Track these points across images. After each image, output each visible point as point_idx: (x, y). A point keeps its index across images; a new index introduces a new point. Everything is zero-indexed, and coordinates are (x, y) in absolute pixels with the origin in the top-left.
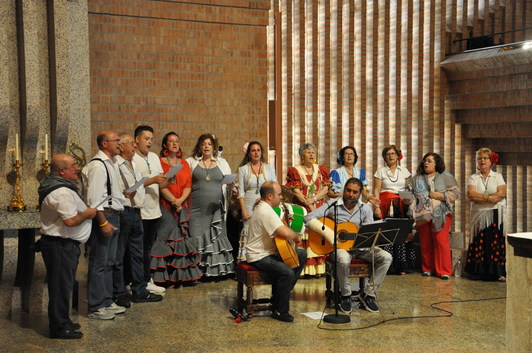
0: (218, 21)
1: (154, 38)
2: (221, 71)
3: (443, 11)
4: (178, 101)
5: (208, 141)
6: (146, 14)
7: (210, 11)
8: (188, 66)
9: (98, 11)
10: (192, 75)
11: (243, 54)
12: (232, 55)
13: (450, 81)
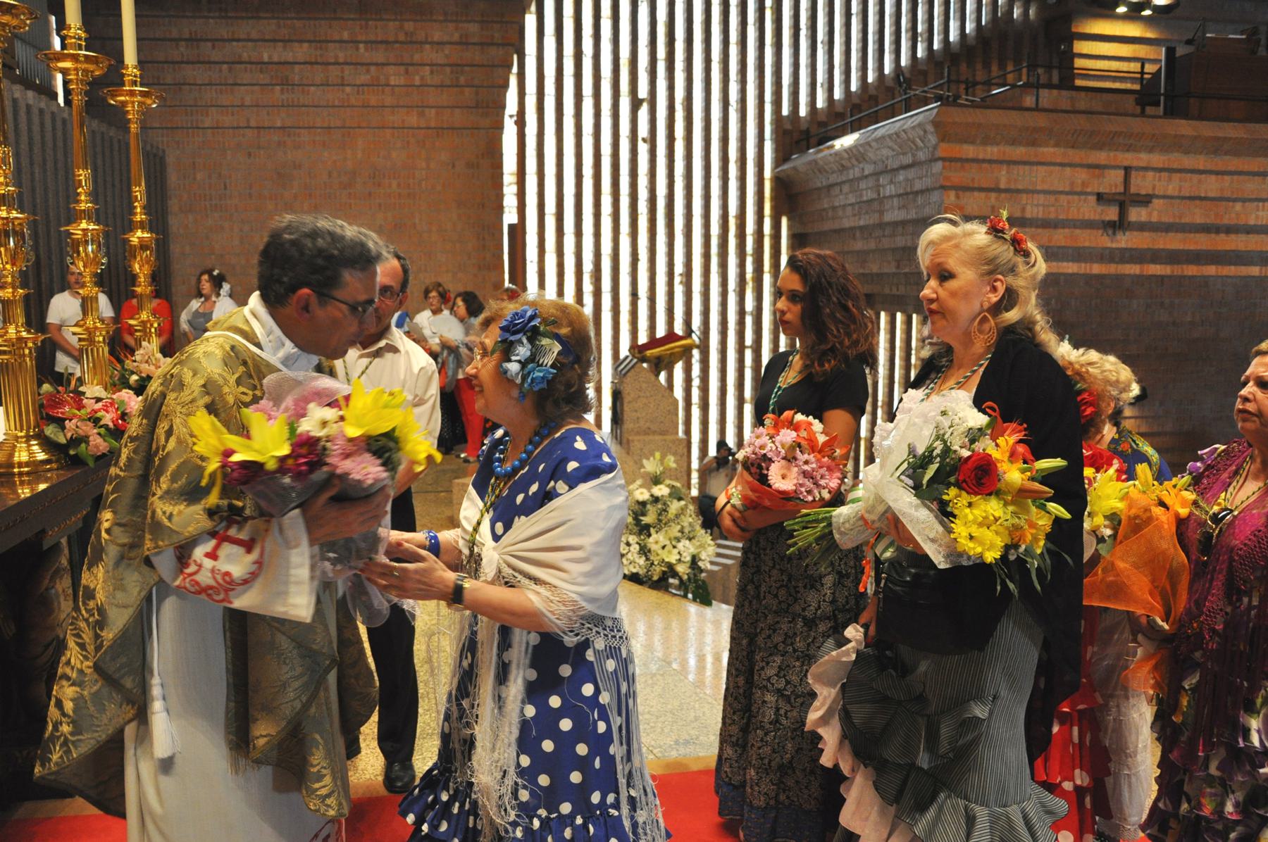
0: (433, 125)
1: (349, 152)
3: (777, 103)
6: (339, 123)
7: (421, 114)
8: (394, 183)
9: (279, 124)
10: (400, 194)
11: (470, 165)
12: (454, 166)
13: (789, 196)
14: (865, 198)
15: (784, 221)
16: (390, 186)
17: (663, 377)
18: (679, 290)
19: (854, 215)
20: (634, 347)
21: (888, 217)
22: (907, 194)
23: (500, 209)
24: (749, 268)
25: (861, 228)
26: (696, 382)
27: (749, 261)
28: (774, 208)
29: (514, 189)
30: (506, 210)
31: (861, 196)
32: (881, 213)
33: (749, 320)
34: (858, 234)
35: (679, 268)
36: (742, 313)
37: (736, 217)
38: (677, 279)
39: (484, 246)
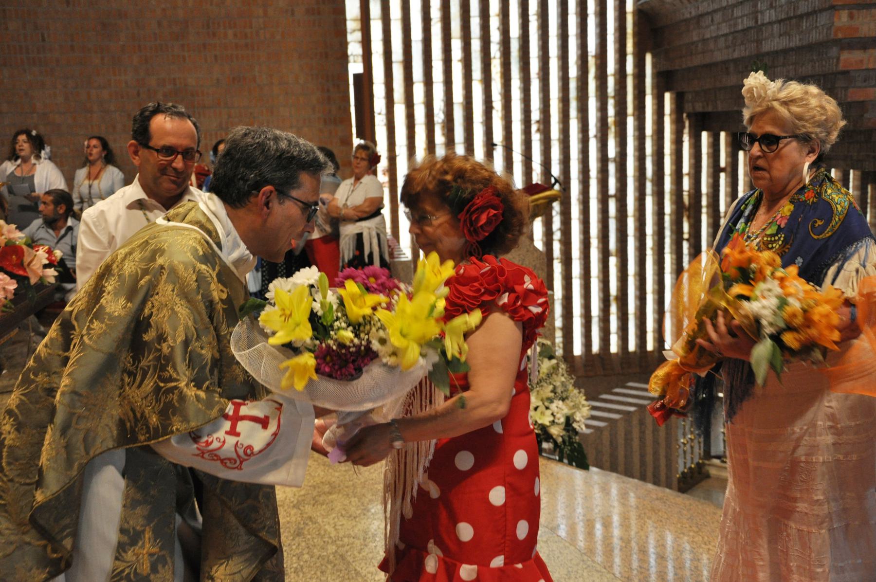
2: (278, 37)
4: (218, 80)
5: (23, 138)
8: (230, 33)
12: (293, 14)
14: (740, 27)
15: (649, 58)
16: (226, 35)
18: (536, 138)
19: (727, 47)
21: (767, 47)
22: (790, 18)
23: (344, 58)
24: (611, 111)
25: (735, 61)
26: (557, 236)
27: (611, 103)
28: (636, 45)
29: (358, 35)
30: (351, 59)
31: (736, 25)
32: (759, 42)
33: (612, 168)
34: (732, 67)
35: (535, 115)
36: (604, 160)
37: (596, 57)
38: (534, 127)
39: (329, 98)
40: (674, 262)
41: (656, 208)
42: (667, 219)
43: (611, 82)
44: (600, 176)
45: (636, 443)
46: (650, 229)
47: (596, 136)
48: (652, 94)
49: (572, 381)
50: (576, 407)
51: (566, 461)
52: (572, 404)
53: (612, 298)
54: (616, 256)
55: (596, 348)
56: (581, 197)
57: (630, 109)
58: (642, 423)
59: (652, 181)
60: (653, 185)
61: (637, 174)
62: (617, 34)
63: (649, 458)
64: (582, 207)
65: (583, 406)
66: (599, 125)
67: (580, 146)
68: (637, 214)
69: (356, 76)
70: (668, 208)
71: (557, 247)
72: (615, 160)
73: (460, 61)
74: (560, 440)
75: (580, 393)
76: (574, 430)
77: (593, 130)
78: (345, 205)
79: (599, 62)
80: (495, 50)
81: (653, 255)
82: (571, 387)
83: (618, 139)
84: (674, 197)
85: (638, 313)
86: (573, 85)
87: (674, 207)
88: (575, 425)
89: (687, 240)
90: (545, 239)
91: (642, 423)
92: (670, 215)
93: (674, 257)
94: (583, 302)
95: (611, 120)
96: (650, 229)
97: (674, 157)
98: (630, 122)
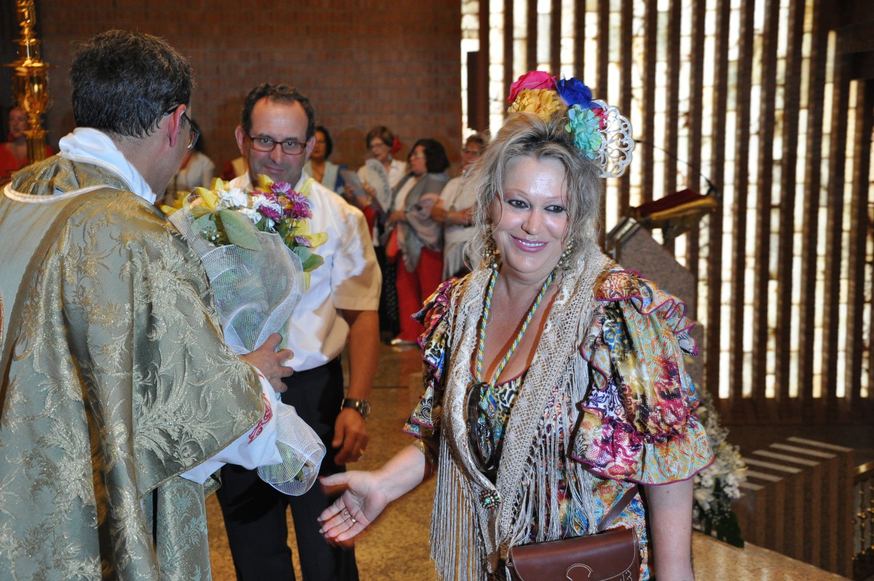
15: (832, 38)
17: (681, 243)
18: (683, 133)
20: (625, 210)
23: (457, 34)
24: (779, 103)
26: (704, 252)
27: (780, 92)
30: (465, 34)
33: (777, 172)
35: (684, 106)
36: (767, 161)
38: (682, 121)
40: (852, 289)
41: (831, 223)
42: (845, 236)
43: (781, 67)
44: (761, 181)
45: (799, 513)
46: (822, 248)
47: (758, 133)
48: (834, 82)
49: (725, 435)
50: (730, 467)
51: (714, 533)
52: (725, 463)
53: (770, 331)
54: (778, 279)
55: (747, 389)
56: (736, 207)
57: (804, 100)
58: (807, 489)
59: (828, 189)
60: (829, 194)
61: (809, 180)
62: (793, 8)
63: (816, 533)
64: (736, 219)
65: (738, 466)
66: (763, 119)
67: (739, 144)
68: (807, 229)
69: (471, 55)
70: (847, 223)
71: (703, 266)
72: (781, 162)
73: (595, 39)
74: (707, 507)
75: (734, 450)
76: (726, 496)
77: (755, 126)
78: (452, 207)
79: (767, 42)
80: (638, 27)
81: (826, 280)
82: (722, 442)
83: (786, 137)
84: (856, 210)
85: (803, 350)
86: (733, 70)
87: (855, 222)
88: (727, 490)
89: (871, 263)
90: (689, 256)
91: (807, 489)
92: (850, 232)
93: (853, 283)
94: (733, 333)
95: (778, 114)
96: (822, 248)
97: (858, 161)
98: (803, 116)
